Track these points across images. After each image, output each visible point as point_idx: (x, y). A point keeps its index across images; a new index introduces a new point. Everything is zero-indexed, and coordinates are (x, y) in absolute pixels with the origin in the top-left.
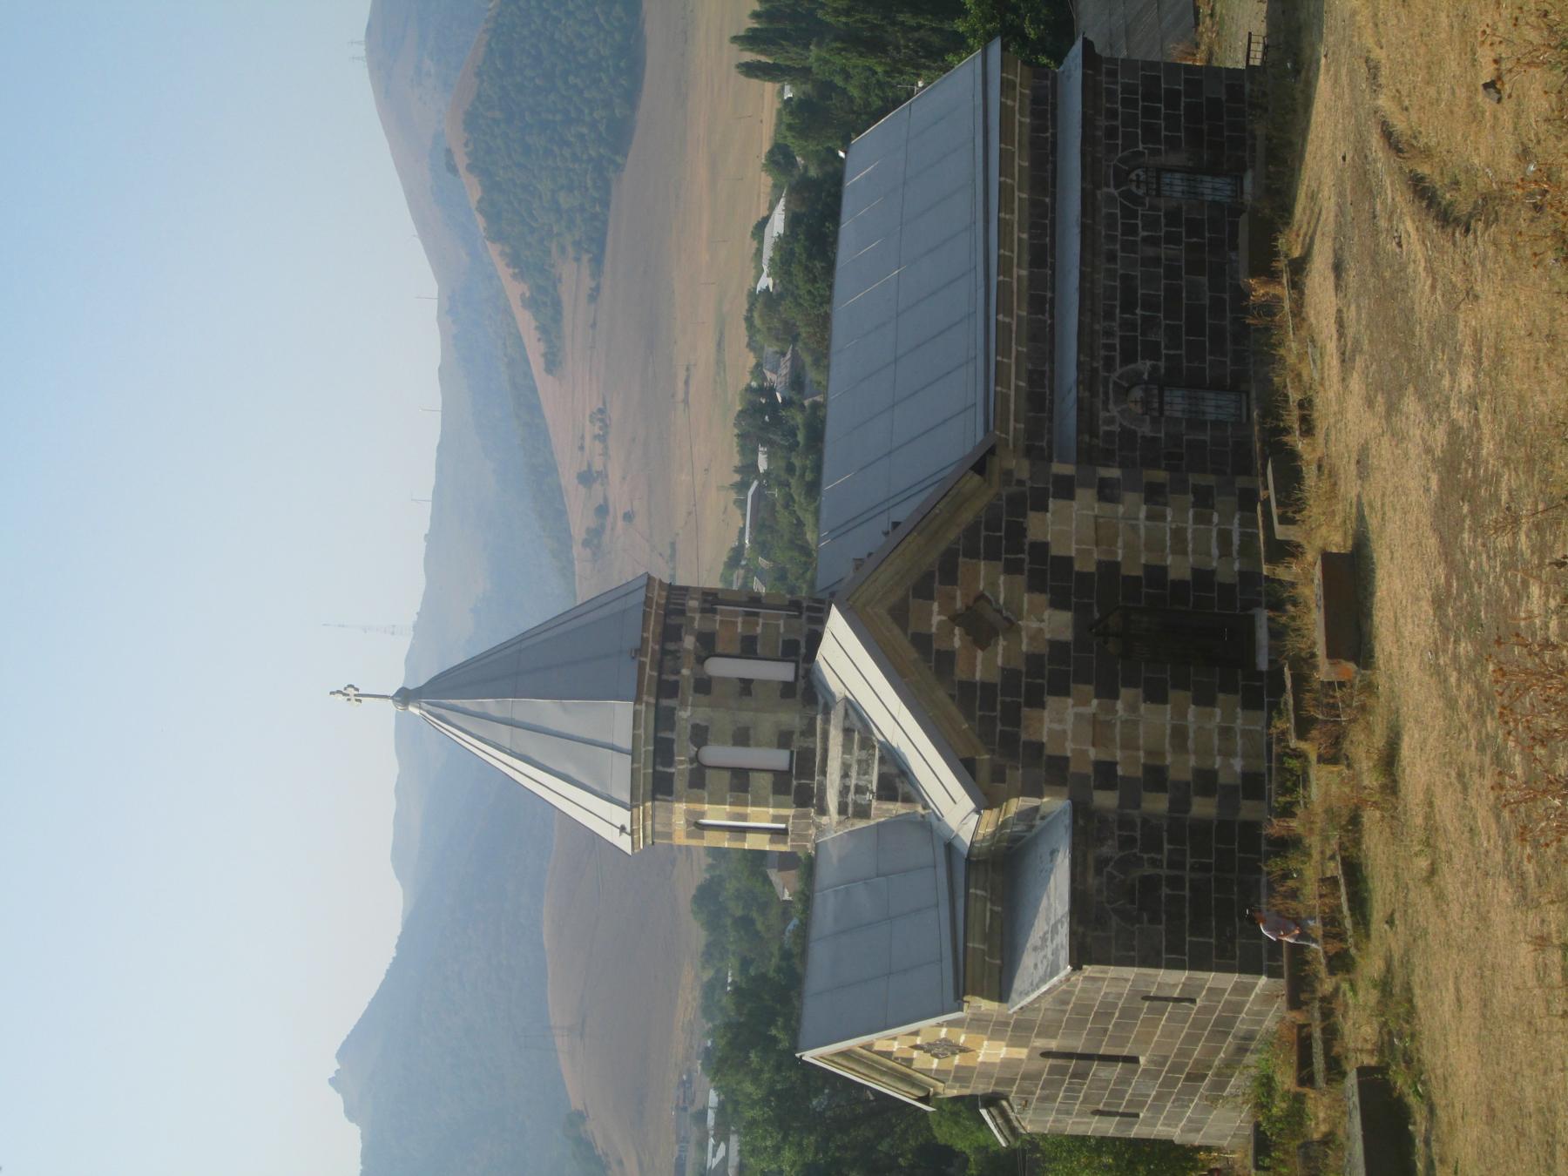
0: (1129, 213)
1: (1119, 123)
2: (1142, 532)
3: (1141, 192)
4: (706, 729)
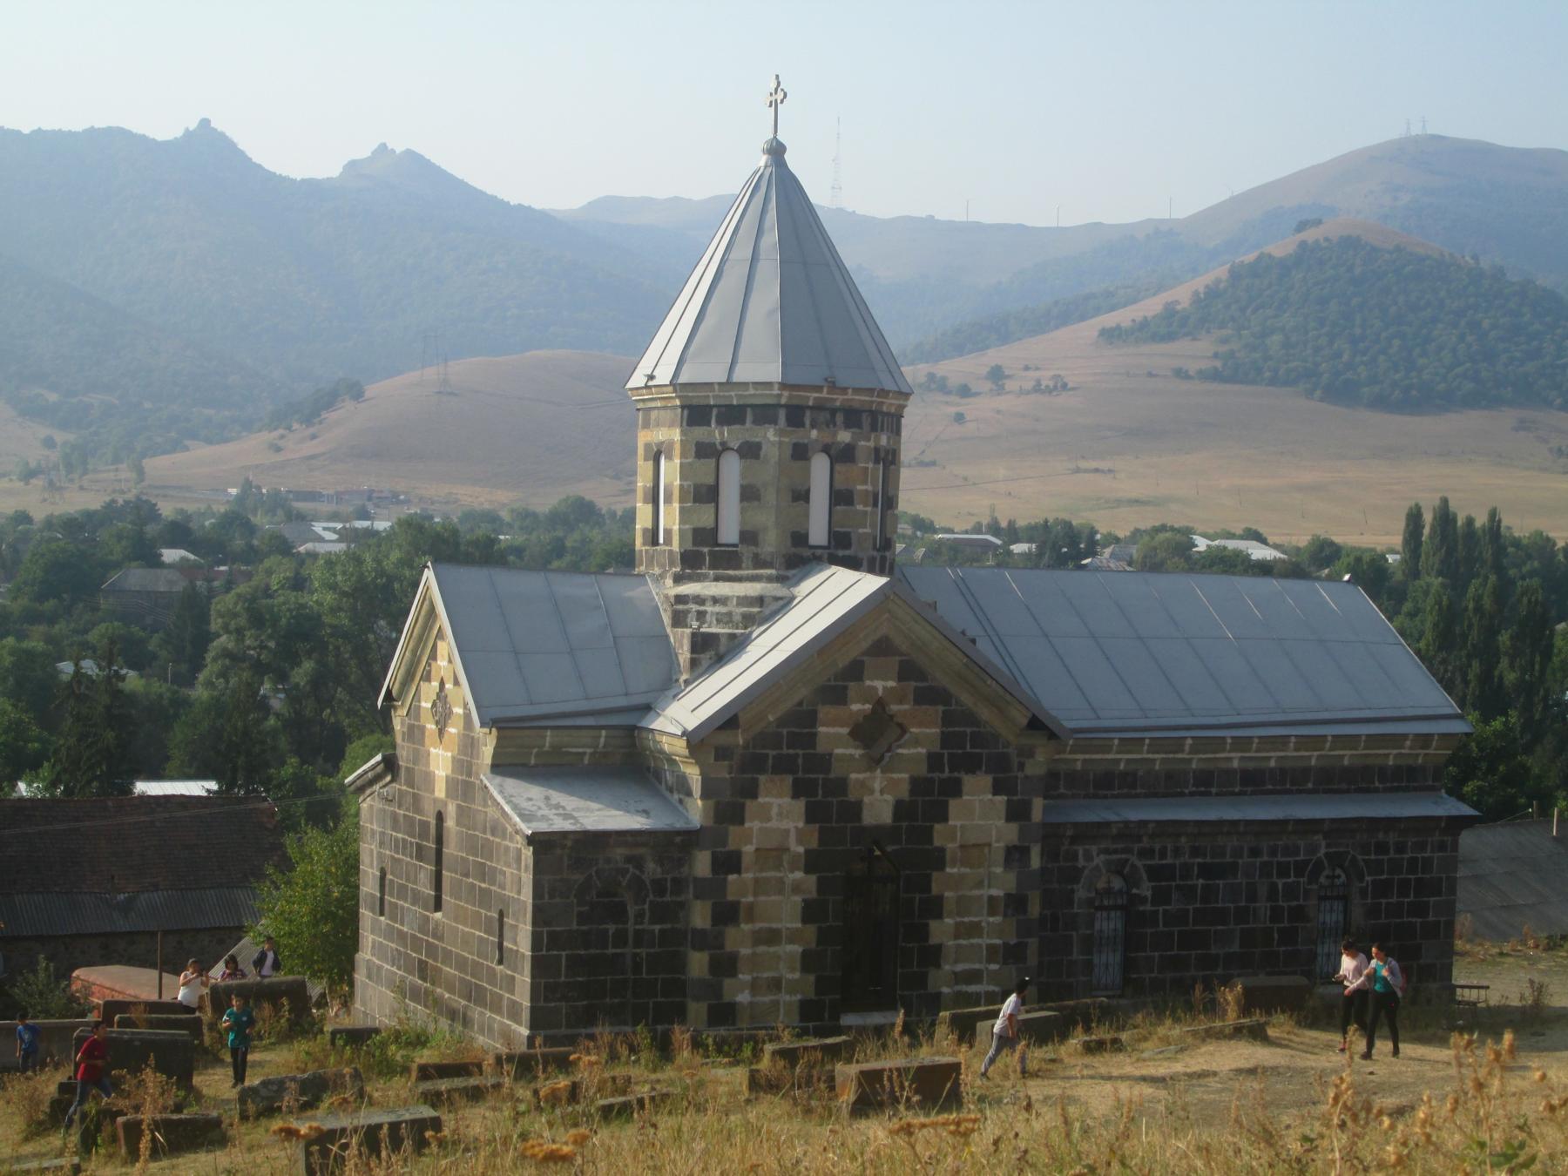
0: (1300, 868)
1: (1392, 855)
2: (976, 892)
3: (1322, 880)
4: (757, 457)
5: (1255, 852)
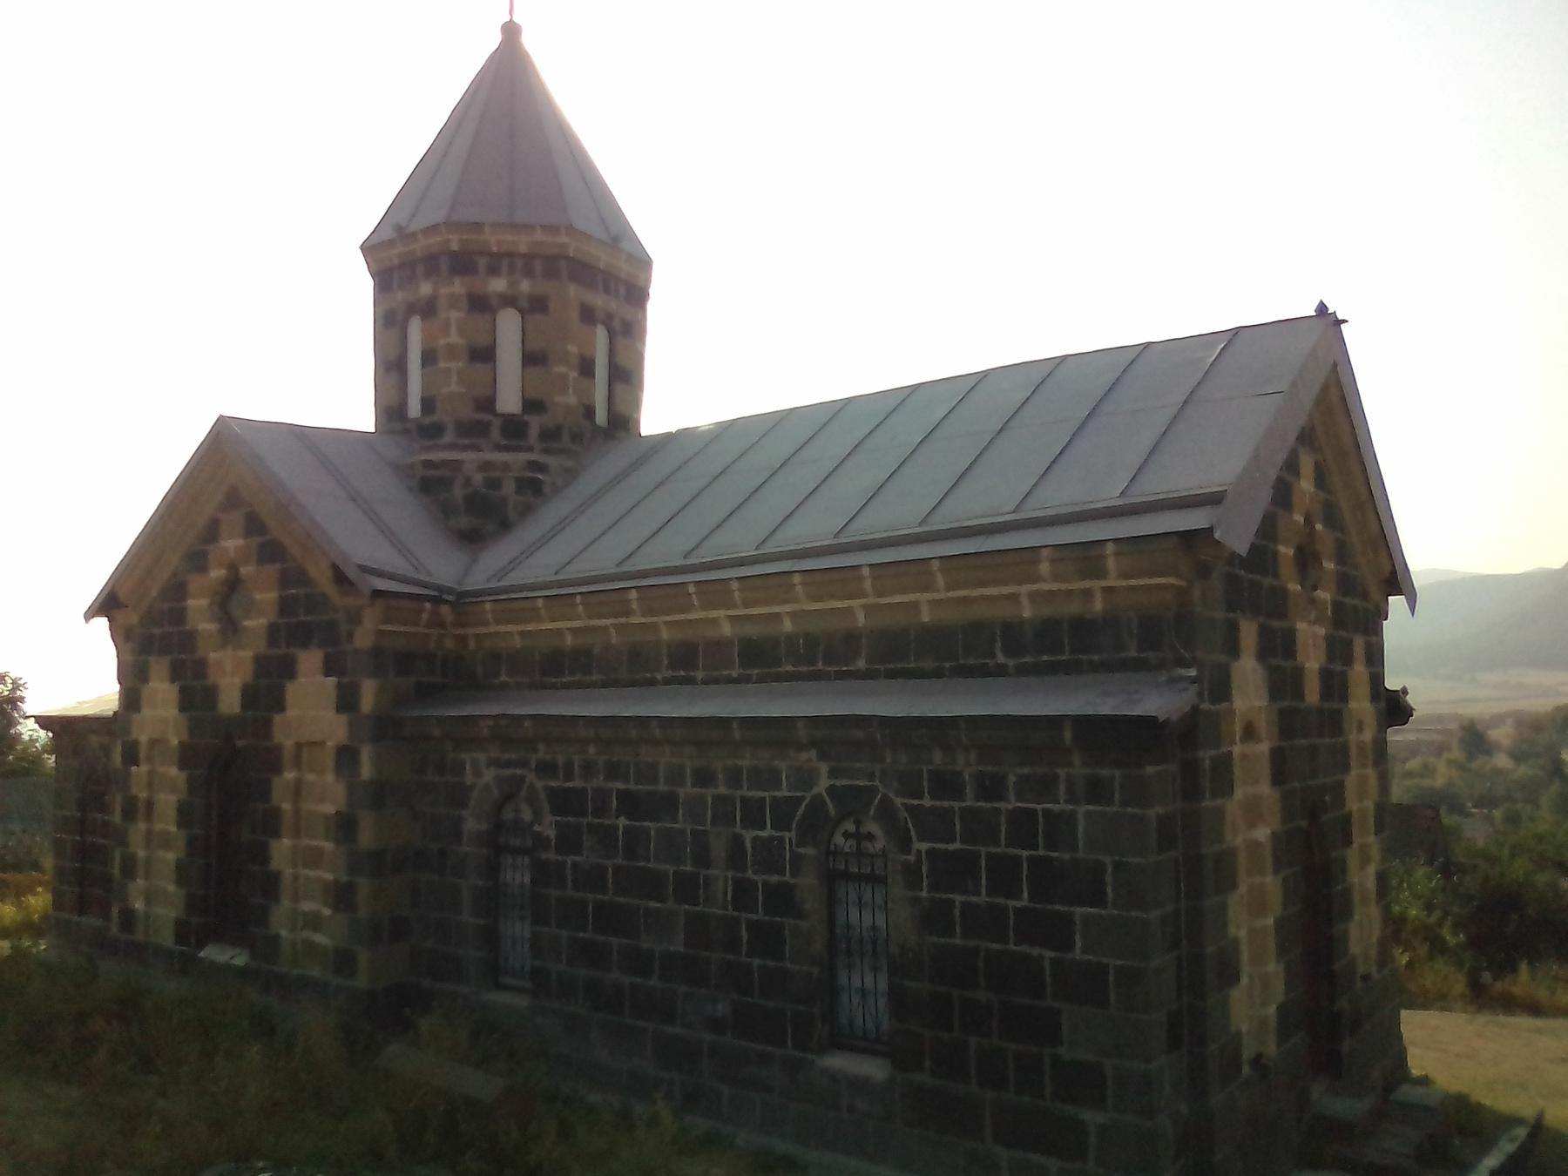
0: (782, 813)
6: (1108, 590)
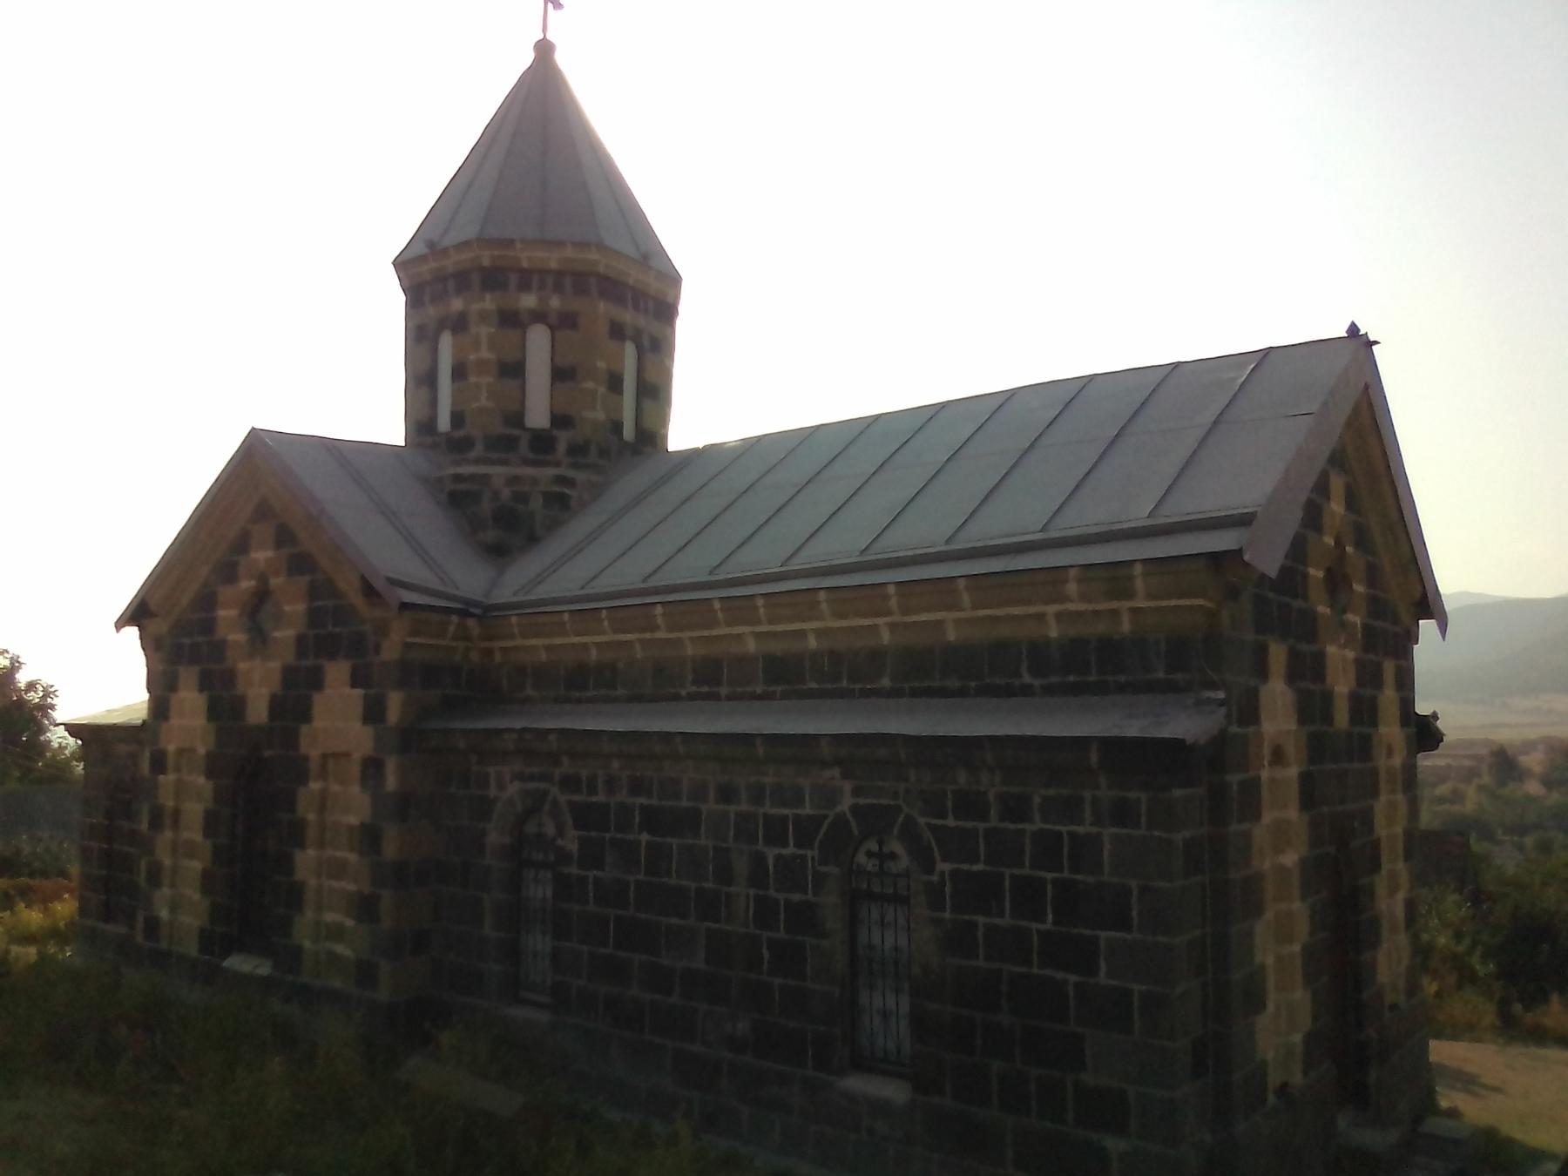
0: (806, 830)
1: (994, 822)
5: (727, 794)
6: (1135, 611)
